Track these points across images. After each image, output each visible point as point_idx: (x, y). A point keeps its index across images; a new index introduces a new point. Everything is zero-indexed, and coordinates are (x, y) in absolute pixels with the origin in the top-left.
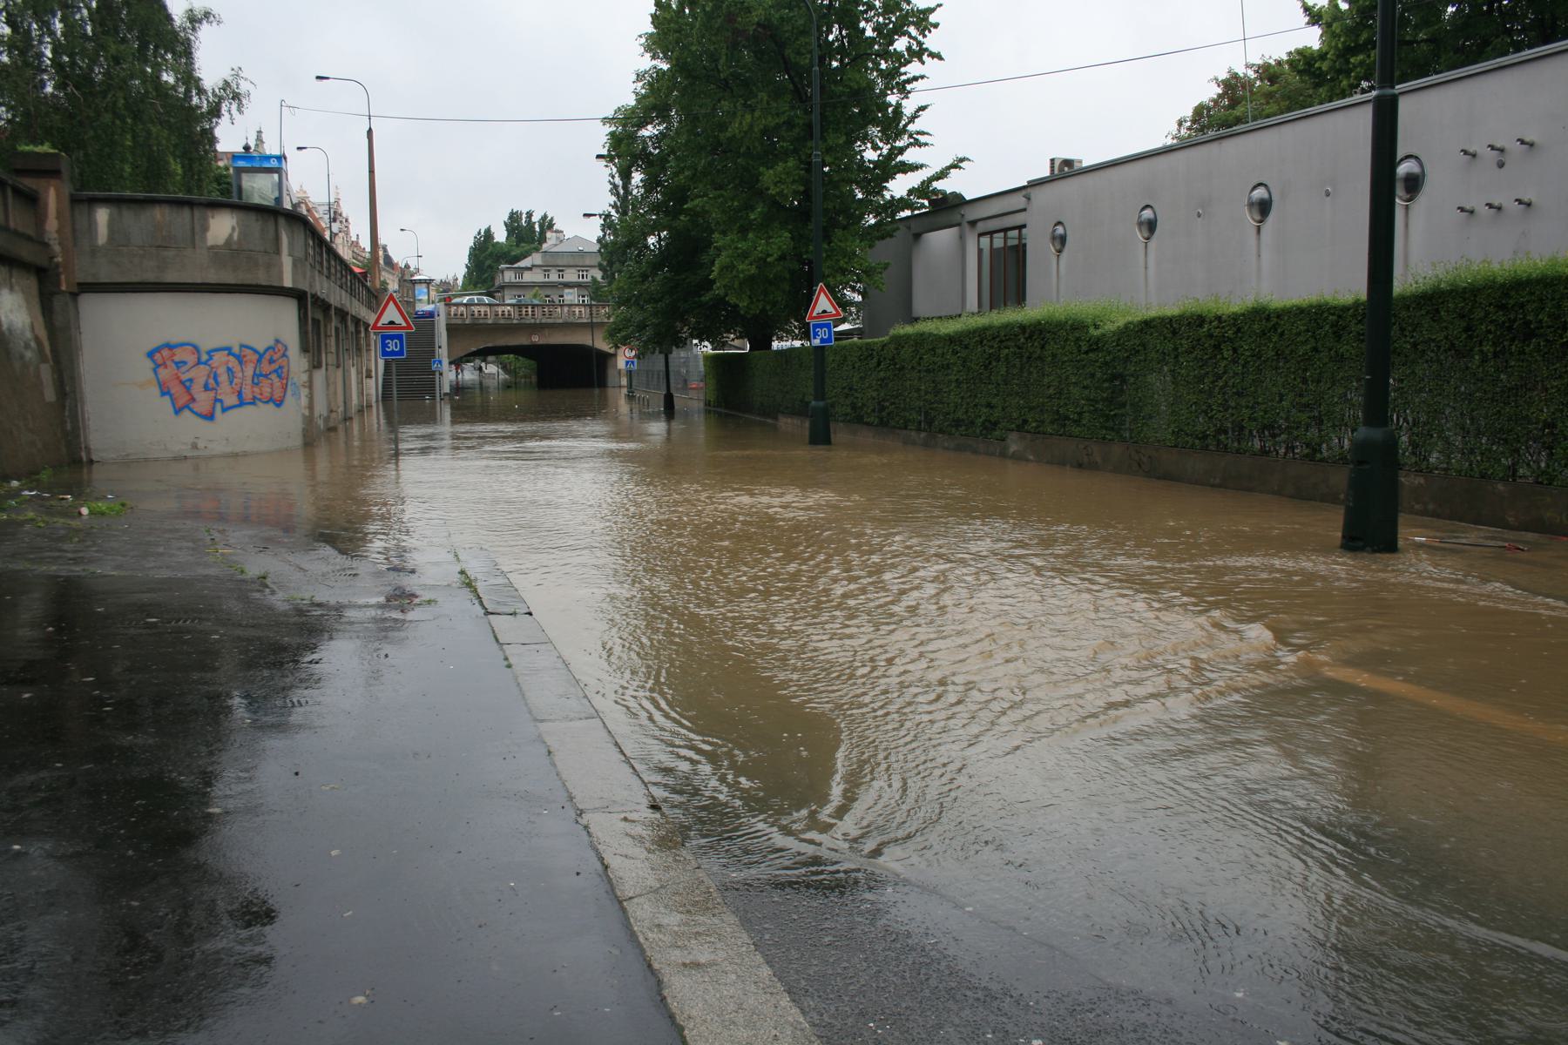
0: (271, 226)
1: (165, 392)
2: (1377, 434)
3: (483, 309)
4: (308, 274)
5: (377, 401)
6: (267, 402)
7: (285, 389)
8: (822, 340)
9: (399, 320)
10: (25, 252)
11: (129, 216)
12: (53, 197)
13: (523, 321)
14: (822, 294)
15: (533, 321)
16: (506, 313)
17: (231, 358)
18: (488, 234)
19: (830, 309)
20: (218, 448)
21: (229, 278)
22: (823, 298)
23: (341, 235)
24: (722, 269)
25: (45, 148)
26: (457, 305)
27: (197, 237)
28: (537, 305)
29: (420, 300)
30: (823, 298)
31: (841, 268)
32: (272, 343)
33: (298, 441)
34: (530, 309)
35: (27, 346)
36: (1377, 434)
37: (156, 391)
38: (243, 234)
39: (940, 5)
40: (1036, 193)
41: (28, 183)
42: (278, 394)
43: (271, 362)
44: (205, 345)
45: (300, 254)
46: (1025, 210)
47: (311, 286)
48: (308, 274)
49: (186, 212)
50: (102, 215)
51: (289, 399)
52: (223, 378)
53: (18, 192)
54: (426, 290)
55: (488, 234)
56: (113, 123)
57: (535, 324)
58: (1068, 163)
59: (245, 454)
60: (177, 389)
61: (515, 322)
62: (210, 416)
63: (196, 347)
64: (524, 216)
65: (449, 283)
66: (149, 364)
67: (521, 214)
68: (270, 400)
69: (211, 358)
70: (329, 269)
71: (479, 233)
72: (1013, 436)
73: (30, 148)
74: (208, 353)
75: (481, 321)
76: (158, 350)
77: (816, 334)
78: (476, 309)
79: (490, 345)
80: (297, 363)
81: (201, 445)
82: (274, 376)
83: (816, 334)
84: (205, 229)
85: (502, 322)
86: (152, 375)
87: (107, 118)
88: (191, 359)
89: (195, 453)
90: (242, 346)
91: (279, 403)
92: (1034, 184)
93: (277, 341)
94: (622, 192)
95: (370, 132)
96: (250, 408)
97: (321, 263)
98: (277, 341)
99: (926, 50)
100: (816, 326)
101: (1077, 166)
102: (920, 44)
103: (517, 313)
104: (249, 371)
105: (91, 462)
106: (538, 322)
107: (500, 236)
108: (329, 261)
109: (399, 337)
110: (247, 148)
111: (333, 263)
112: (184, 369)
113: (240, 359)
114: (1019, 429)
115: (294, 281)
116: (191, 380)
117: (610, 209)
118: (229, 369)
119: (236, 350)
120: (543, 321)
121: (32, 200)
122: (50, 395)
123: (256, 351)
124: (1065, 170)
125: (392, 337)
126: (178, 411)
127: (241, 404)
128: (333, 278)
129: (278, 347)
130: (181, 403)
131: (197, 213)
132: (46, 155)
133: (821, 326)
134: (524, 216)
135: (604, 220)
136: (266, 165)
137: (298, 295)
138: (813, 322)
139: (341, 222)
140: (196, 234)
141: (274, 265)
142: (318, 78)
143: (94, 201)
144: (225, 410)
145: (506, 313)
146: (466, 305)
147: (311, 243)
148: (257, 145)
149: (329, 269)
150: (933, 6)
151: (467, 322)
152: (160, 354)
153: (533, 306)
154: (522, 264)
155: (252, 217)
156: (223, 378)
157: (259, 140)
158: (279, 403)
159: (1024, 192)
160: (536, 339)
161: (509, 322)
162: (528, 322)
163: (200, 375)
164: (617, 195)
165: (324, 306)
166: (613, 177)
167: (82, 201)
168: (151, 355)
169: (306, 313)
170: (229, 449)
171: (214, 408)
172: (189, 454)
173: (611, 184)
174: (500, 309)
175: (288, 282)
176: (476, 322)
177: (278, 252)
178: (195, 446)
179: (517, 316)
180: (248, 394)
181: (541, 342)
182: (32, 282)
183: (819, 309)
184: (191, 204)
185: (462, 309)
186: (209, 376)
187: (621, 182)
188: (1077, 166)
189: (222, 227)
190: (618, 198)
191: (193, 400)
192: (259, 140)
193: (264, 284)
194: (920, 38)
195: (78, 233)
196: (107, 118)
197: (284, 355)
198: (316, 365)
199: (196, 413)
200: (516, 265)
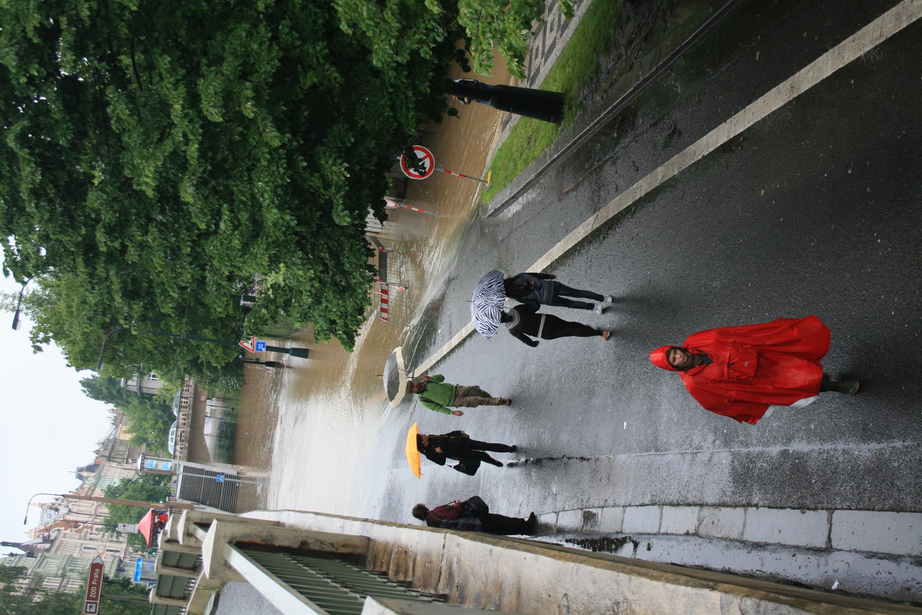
13: (191, 406)
16: (184, 417)
18: (86, 384)
23: (70, 507)
24: (217, 362)
29: (156, 466)
34: (183, 400)
54: (149, 461)
55: (86, 384)
57: (194, 398)
61: (191, 412)
65: (115, 417)
71: (84, 391)
75: (188, 436)
77: (261, 350)
85: (190, 421)
100: (257, 349)
103: (185, 410)
106: (192, 396)
107: (88, 374)
133: (257, 347)
139: (60, 505)
142: (25, 523)
145: (184, 417)
151: (187, 445)
153: (182, 397)
161: (190, 416)
179: (186, 410)
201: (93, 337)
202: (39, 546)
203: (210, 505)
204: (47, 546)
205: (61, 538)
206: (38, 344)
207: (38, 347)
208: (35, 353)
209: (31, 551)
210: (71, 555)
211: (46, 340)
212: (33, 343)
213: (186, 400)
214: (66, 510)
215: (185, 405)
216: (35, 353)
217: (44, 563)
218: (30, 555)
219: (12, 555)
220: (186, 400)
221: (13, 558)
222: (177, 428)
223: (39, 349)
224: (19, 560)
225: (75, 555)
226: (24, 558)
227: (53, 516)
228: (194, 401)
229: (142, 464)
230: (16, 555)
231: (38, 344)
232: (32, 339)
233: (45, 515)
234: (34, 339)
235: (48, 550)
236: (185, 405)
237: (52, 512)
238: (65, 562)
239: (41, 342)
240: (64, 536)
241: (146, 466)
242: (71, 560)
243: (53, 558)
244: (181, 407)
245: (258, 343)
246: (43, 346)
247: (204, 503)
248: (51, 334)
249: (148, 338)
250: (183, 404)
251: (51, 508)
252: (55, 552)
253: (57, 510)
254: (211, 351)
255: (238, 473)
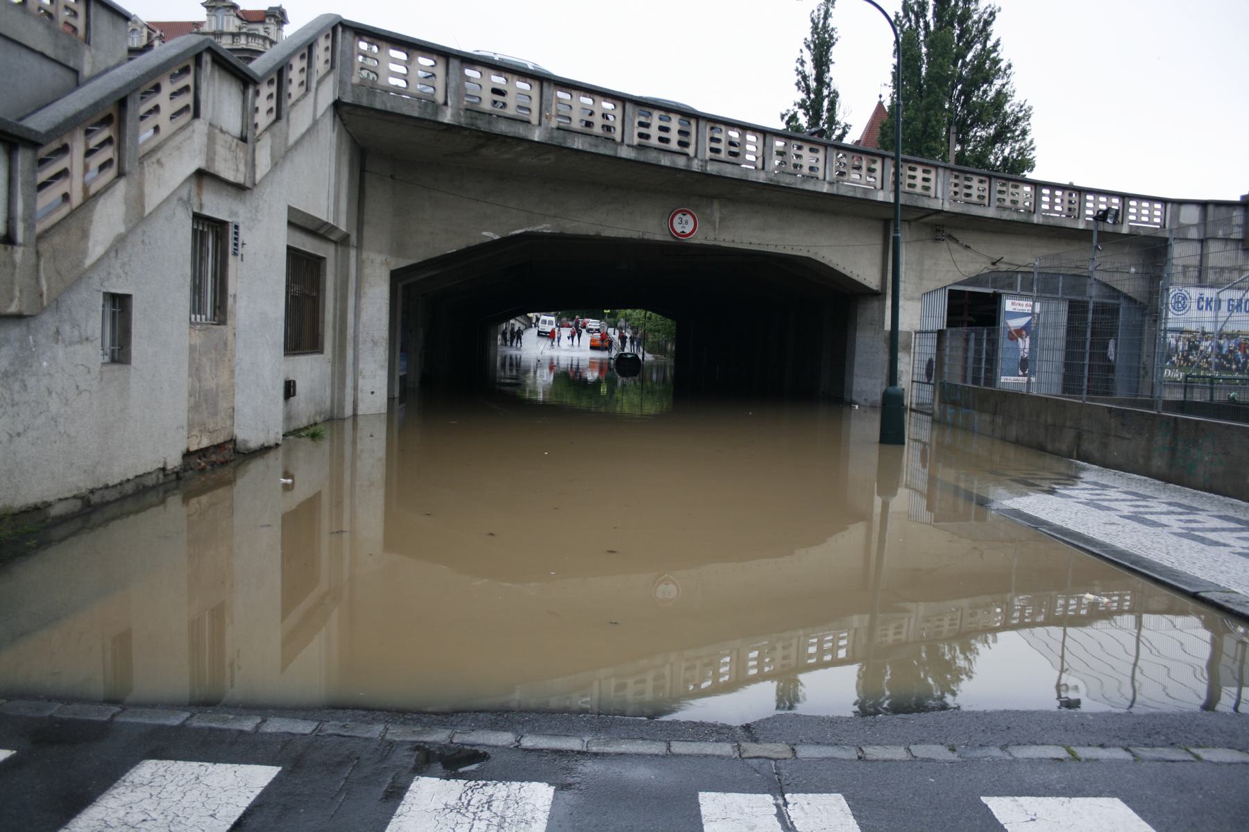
13: (652, 157)
15: (681, 162)
34: (675, 124)
57: (688, 172)
61: (624, 153)
75: (503, 128)
79: (545, 227)
85: (578, 144)
94: (813, 84)
117: (796, 108)
120: (712, 168)
135: (788, 123)
145: (598, 121)
151: (447, 117)
160: (684, 225)
161: (602, 150)
162: (666, 161)
164: (808, 90)
166: (802, 63)
173: (800, 73)
176: (482, 125)
181: (698, 239)
187: (814, 72)
190: (808, 94)
215: (654, 132)
220: (674, 137)
236: (654, 132)
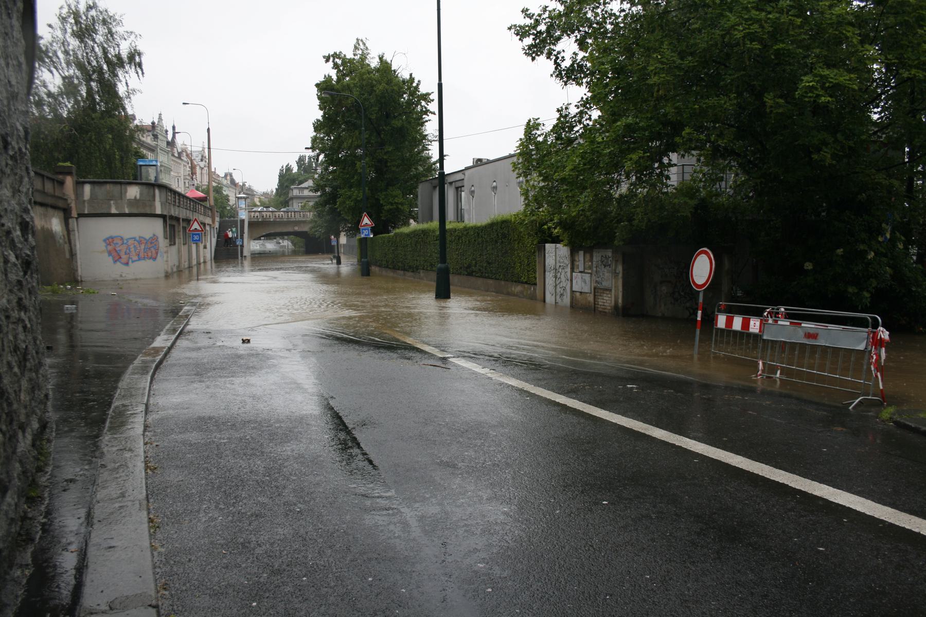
0: (152, 190)
1: (110, 253)
2: (443, 266)
3: (268, 214)
4: (168, 207)
5: (211, 260)
6: (150, 259)
7: (157, 253)
8: (366, 235)
9: (199, 228)
10: (61, 204)
11: (97, 188)
12: (69, 181)
14: (366, 217)
17: (136, 242)
18: (289, 169)
19: (369, 223)
20: (130, 277)
21: (135, 211)
22: (366, 217)
25: (68, 164)
26: (255, 212)
27: (123, 196)
28: (297, 212)
30: (366, 218)
31: (390, 202)
32: (151, 235)
33: (163, 275)
34: (293, 214)
35: (60, 238)
36: (443, 266)
37: (106, 254)
38: (141, 194)
39: (433, 93)
40: (467, 172)
41: (61, 177)
42: (154, 255)
43: (151, 243)
44: (126, 236)
45: (164, 200)
46: (463, 179)
47: (169, 213)
48: (168, 207)
49: (118, 187)
50: (87, 188)
51: (159, 258)
52: (132, 249)
53: (58, 182)
54: (244, 202)
55: (289, 169)
56: (91, 145)
58: (480, 160)
59: (140, 279)
60: (114, 254)
62: (127, 264)
63: (122, 239)
64: (307, 158)
65: (268, 194)
66: (105, 244)
67: (305, 157)
68: (150, 259)
69: (128, 242)
70: (179, 203)
71: (282, 167)
72: (421, 271)
73: (61, 164)
74: (127, 240)
75: (267, 220)
76: (108, 239)
78: (264, 214)
79: (272, 232)
80: (163, 243)
81: (123, 275)
82: (152, 249)
83: (363, 233)
84: (126, 192)
86: (105, 248)
87: (88, 143)
88: (120, 242)
89: (122, 278)
90: (140, 237)
91: (155, 259)
92: (467, 168)
93: (154, 235)
95: (208, 130)
96: (143, 261)
97: (175, 202)
98: (154, 235)
99: (428, 110)
101: (484, 161)
102: (426, 108)
104: (143, 247)
105: (82, 281)
106: (297, 220)
107: (295, 169)
108: (179, 200)
109: (199, 234)
110: (153, 123)
111: (182, 199)
112: (117, 246)
113: (140, 242)
114: (423, 269)
115: (162, 211)
116: (120, 250)
118: (135, 247)
119: (138, 239)
121: (62, 183)
122: (68, 256)
123: (145, 239)
124: (479, 162)
125: (196, 234)
126: (115, 261)
127: (139, 259)
128: (182, 206)
129: (154, 238)
130: (117, 258)
131: (123, 186)
132: (68, 166)
133: (365, 229)
134: (307, 158)
136: (151, 164)
137: (163, 216)
138: (361, 228)
139: (206, 161)
140: (122, 195)
141: (153, 206)
142: (184, 103)
143: (84, 183)
144: (133, 262)
146: (259, 212)
147: (170, 194)
148: (159, 121)
149: (179, 203)
150: (430, 92)
151: (260, 220)
152: (109, 241)
153: (295, 212)
154: (303, 186)
155: (144, 187)
156: (132, 249)
157: (160, 119)
158: (155, 259)
159: (463, 172)
160: (296, 228)
161: (282, 220)
162: (292, 220)
163: (124, 248)
165: (177, 219)
167: (79, 184)
168: (105, 241)
169: (166, 224)
170: (134, 277)
171: (129, 260)
172: (119, 279)
174: (277, 214)
175: (158, 211)
177: (154, 200)
178: (121, 276)
180: (142, 255)
182: (61, 214)
183: (364, 223)
184: (121, 183)
185: (257, 214)
186: (127, 249)
188: (484, 161)
189: (133, 192)
191: (120, 258)
192: (160, 119)
193: (149, 213)
194: (426, 106)
195: (78, 194)
196: (88, 143)
197: (157, 240)
198: (172, 243)
199: (121, 263)
200: (299, 186)
201: (346, 94)
202: (175, 149)
203: (217, 241)
204: (176, 155)
205: (183, 163)
206: (331, 59)
207: (329, 58)
208: (324, 57)
209: (171, 144)
210: (171, 170)
211: (336, 66)
212: (332, 56)
213: (293, 216)
214: (202, 166)
216: (324, 57)
217: (163, 152)
218: (168, 143)
219: (167, 131)
220: (293, 216)
221: (164, 132)
222: (272, 212)
223: (327, 59)
224: (164, 137)
225: (172, 173)
226: (165, 139)
227: (197, 158)
228: (293, 222)
229: (241, 198)
230: (167, 134)
231: (331, 59)
232: (335, 53)
233: (197, 153)
234: (335, 55)
235: (173, 155)
237: (200, 157)
238: (167, 166)
239: (333, 61)
240: (184, 166)
241: (240, 200)
242: (168, 170)
243: (168, 158)
244: (288, 212)
245: (368, 229)
246: (331, 64)
247: (218, 238)
248: (341, 68)
249: (352, 141)
250: (290, 214)
251: (202, 156)
252: (172, 160)
253: (202, 160)
254: (350, 197)
255: (245, 257)
